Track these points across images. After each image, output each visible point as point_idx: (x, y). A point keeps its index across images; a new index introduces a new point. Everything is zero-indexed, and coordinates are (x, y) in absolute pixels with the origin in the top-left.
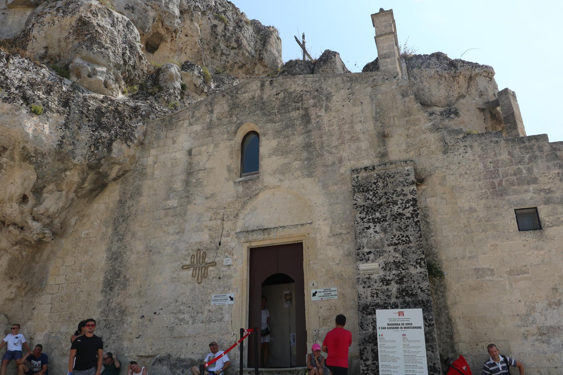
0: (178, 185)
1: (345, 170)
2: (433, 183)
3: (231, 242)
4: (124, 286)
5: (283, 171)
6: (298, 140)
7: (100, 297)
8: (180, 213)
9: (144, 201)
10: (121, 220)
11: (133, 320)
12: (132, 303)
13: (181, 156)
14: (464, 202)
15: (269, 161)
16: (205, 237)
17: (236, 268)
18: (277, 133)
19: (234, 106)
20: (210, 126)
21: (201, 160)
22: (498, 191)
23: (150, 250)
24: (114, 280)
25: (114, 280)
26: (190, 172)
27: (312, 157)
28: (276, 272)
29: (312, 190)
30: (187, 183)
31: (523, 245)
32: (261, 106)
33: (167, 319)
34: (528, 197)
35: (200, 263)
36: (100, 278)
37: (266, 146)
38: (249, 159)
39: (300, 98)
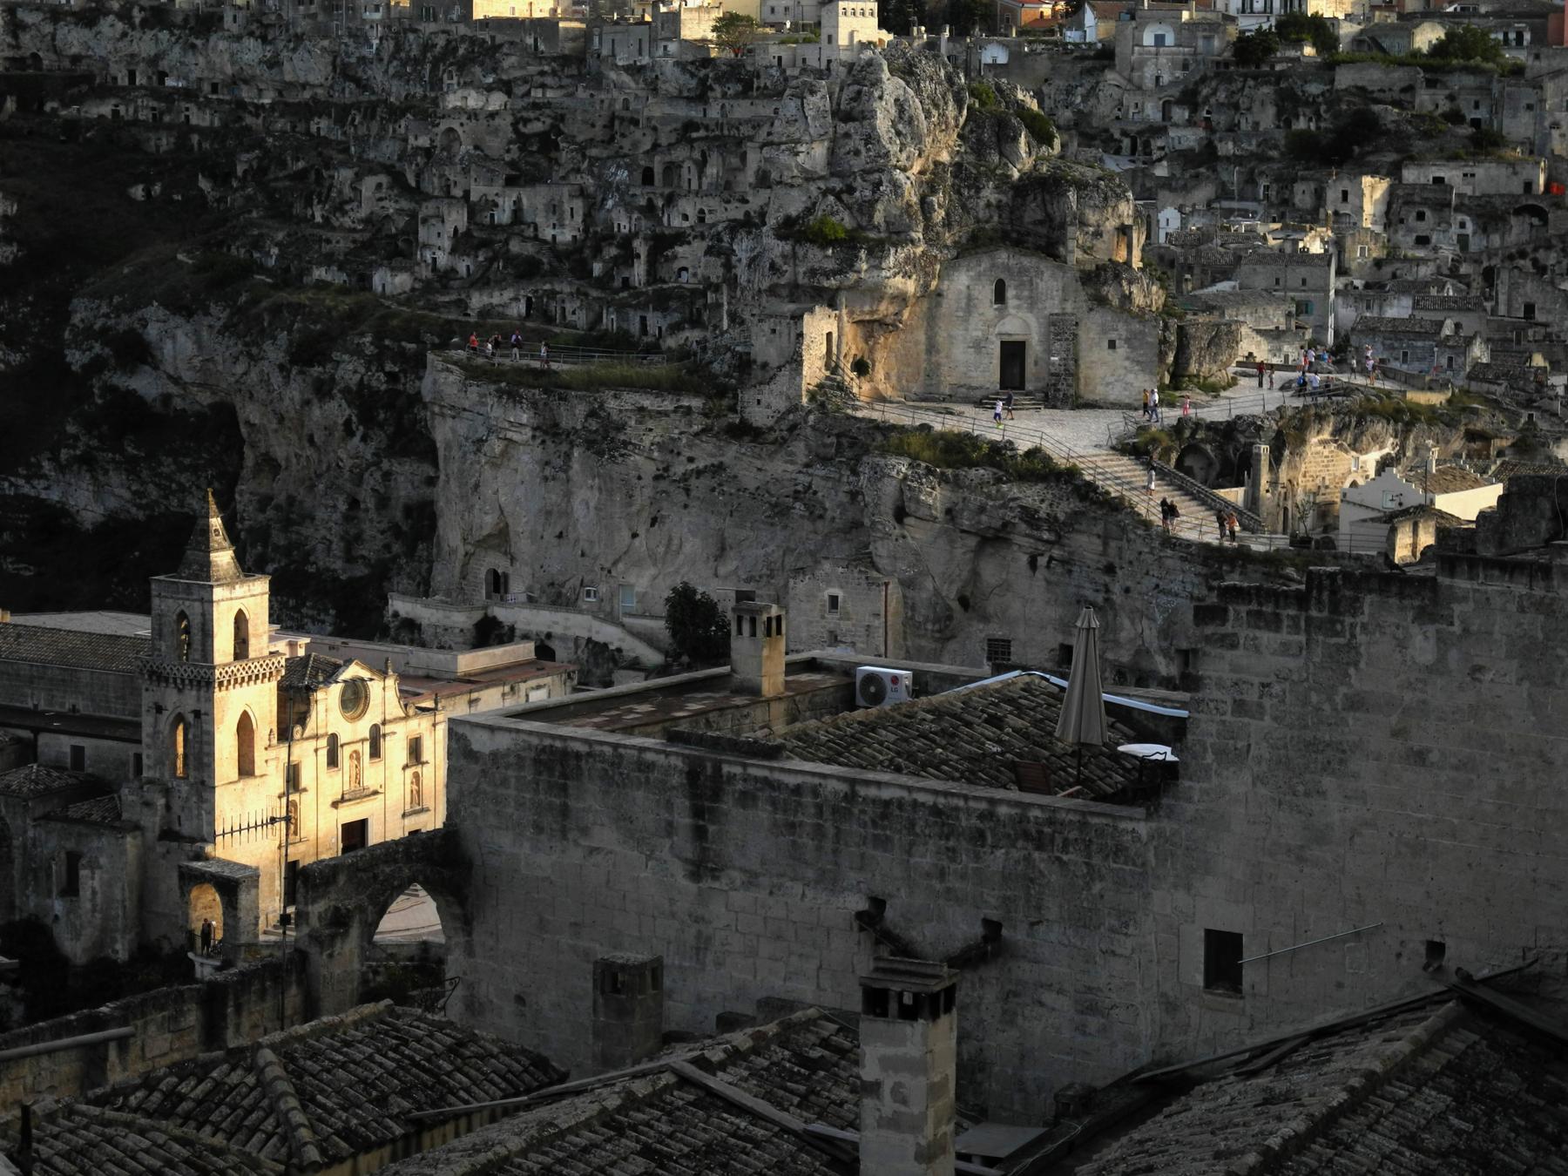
0: (963, 305)
1: (1047, 312)
2: (1082, 325)
3: (993, 338)
4: (938, 352)
5: (1018, 307)
6: (1026, 293)
7: (924, 356)
8: (966, 320)
9: (944, 309)
10: (931, 319)
11: (944, 370)
12: (943, 361)
13: (963, 288)
14: (1091, 335)
15: (1011, 302)
16: (980, 334)
17: (995, 349)
18: (1016, 288)
19: (993, 266)
20: (979, 275)
21: (975, 293)
22: (1104, 332)
23: (950, 336)
24: (932, 348)
25: (932, 348)
26: (969, 298)
27: (1033, 303)
28: (1013, 353)
29: (1032, 320)
30: (968, 305)
31: (1106, 354)
32: (1007, 268)
33: (963, 369)
34: (1113, 336)
35: (978, 346)
36: (922, 347)
37: (1010, 293)
38: (1000, 296)
39: (1027, 270)
